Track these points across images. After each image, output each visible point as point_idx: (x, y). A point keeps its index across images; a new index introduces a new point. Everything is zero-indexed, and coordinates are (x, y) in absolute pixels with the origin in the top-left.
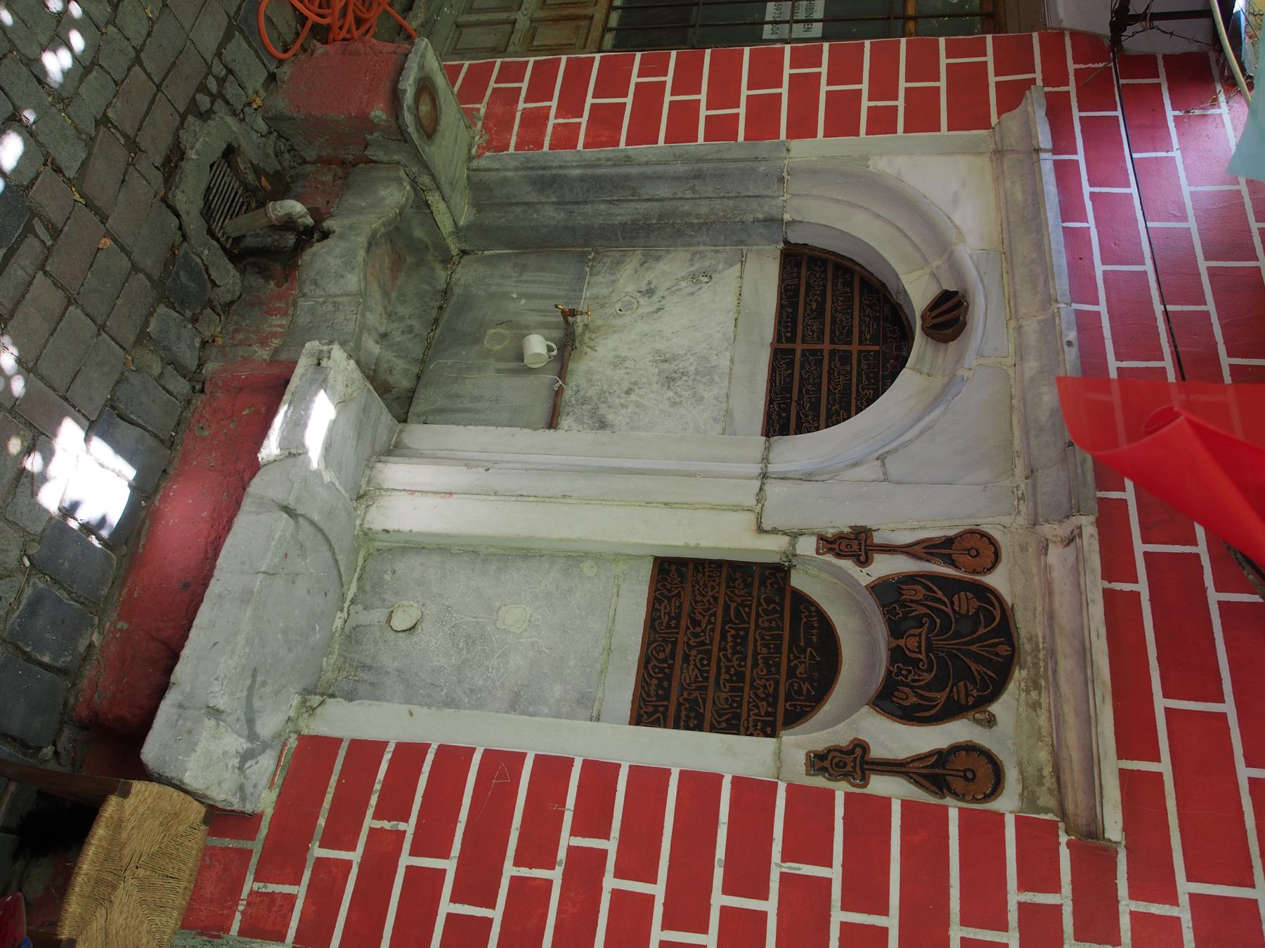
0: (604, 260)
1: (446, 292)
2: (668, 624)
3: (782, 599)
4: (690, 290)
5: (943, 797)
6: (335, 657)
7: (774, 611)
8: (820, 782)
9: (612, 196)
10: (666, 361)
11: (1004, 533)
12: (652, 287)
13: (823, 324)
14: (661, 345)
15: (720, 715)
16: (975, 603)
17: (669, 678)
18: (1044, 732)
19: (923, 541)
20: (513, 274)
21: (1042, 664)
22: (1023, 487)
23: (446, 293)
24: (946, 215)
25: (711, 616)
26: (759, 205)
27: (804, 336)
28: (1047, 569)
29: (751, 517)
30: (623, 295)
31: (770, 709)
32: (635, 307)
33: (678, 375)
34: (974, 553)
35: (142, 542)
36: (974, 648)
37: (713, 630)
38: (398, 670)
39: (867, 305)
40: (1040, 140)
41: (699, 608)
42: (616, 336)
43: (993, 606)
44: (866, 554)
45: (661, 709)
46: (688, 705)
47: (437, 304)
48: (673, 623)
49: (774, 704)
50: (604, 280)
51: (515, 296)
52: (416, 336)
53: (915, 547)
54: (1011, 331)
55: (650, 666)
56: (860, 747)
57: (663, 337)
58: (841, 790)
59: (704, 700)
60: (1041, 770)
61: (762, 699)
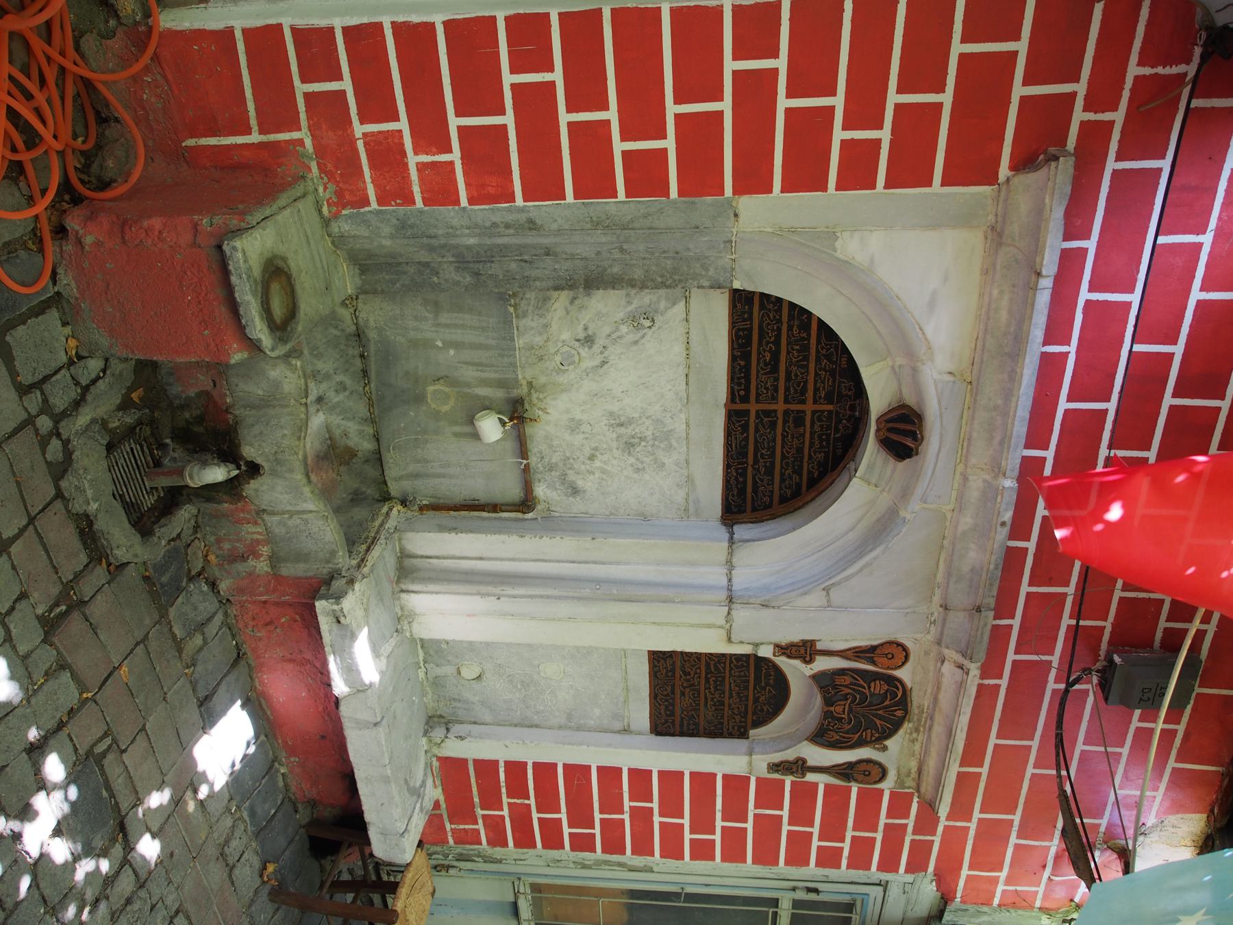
0: (527, 296)
1: (359, 335)
4: (631, 337)
5: (850, 782)
6: (431, 694)
8: (776, 776)
9: (521, 255)
10: (622, 425)
12: (590, 333)
13: (777, 379)
14: (615, 407)
16: (886, 687)
17: (672, 705)
18: (917, 753)
19: (854, 648)
20: (427, 314)
22: (936, 614)
23: (359, 335)
24: (918, 324)
26: (702, 266)
27: (758, 395)
28: (939, 674)
29: (723, 633)
30: (560, 344)
31: (743, 720)
32: (577, 361)
33: (637, 440)
34: (890, 656)
35: (269, 713)
36: (880, 712)
37: (699, 677)
38: (479, 701)
39: (823, 355)
40: (1045, 263)
41: (687, 665)
42: (564, 397)
43: (898, 689)
44: (810, 655)
47: (356, 352)
48: (670, 674)
49: (745, 717)
50: (534, 324)
51: (439, 344)
52: (351, 393)
54: (958, 476)
56: (804, 761)
57: (613, 398)
58: (788, 781)
59: (698, 716)
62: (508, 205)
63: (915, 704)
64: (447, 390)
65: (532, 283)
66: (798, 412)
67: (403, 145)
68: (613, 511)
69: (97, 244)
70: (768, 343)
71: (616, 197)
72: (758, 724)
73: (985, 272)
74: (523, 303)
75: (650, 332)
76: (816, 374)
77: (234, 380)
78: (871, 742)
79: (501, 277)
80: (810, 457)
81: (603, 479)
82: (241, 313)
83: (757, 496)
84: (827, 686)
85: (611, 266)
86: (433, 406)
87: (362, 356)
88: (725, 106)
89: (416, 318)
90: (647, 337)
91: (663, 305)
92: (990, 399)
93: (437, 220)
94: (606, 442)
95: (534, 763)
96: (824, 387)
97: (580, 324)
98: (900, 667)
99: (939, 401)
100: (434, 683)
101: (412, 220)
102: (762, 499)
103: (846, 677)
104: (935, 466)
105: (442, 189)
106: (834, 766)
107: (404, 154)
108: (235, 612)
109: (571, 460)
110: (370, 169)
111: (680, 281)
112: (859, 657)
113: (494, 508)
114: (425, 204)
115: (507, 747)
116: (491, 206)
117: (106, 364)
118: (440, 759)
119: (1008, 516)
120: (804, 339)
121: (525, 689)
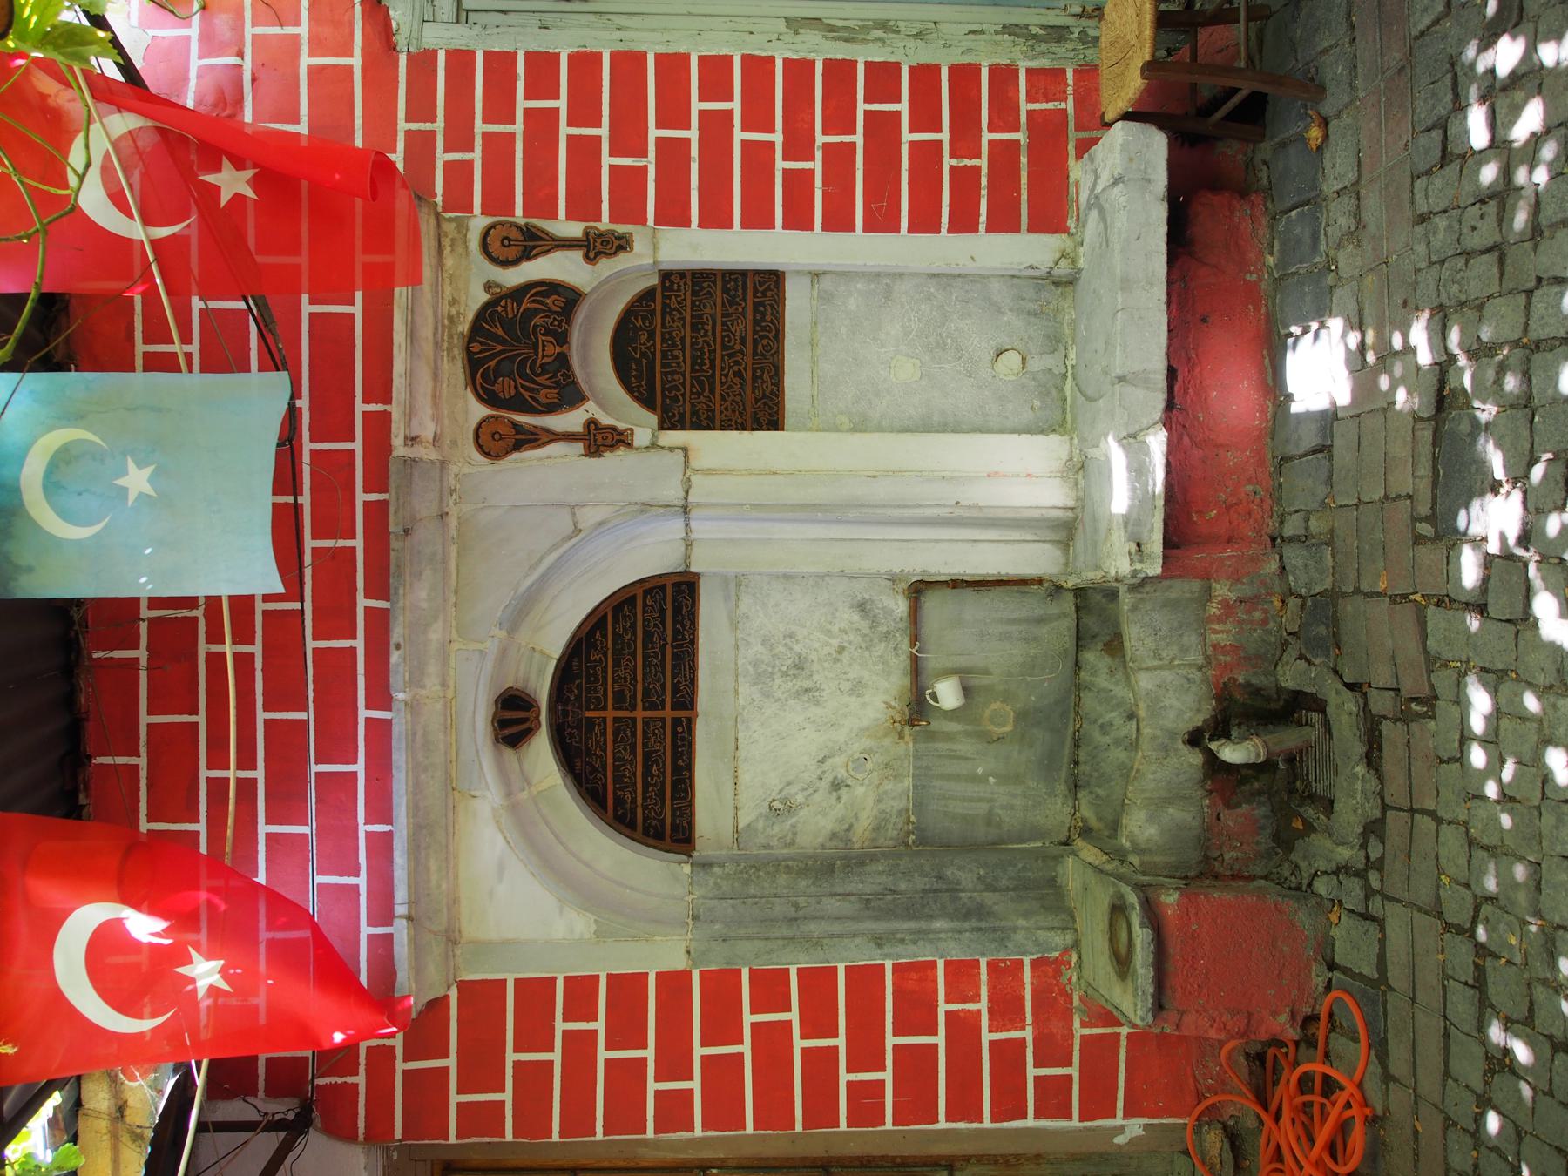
0: (895, 832)
1: (1076, 786)
2: (762, 369)
3: (663, 401)
4: (793, 790)
5: (526, 224)
6: (1066, 321)
7: (670, 390)
8: (621, 229)
9: (894, 899)
10: (806, 690)
11: (470, 458)
12: (835, 794)
13: (645, 745)
14: (815, 711)
15: (709, 293)
16: (496, 387)
17: (756, 323)
18: (447, 281)
19: (539, 446)
20: (1000, 812)
21: (446, 338)
23: (1075, 786)
24: (511, 847)
25: (726, 382)
26: (720, 887)
27: (663, 727)
28: (437, 419)
29: (694, 464)
30: (866, 781)
31: (667, 301)
32: (850, 763)
33: (791, 672)
34: (497, 436)
35: (1267, 360)
36: (499, 348)
37: (723, 369)
38: (1003, 313)
39: (599, 772)
40: (406, 931)
41: (737, 389)
42: (866, 723)
45: (759, 295)
46: (738, 299)
47: (1082, 768)
48: (758, 374)
49: (665, 306)
50: (892, 802)
51: (992, 780)
52: (1096, 721)
53: (546, 440)
54: (452, 684)
55: (774, 332)
56: (590, 259)
57: (814, 721)
58: (605, 223)
60: (452, 251)
61: (675, 309)
62: (900, 961)
63: (459, 363)
64: (991, 727)
65: (887, 869)
66: (620, 708)
67: (990, 1019)
68: (821, 582)
69: (1275, 1013)
70: (655, 785)
71: (798, 969)
72: (647, 296)
73: (456, 901)
74: (900, 826)
75: (774, 795)
76: (605, 751)
77: (1195, 824)
78: (506, 296)
79: (916, 875)
80: (605, 655)
81: (831, 623)
82: (1152, 956)
83: (661, 606)
84: (567, 385)
85: (808, 887)
86: (1008, 708)
87: (1076, 763)
88: (699, 1051)
89: (1012, 807)
90: (776, 790)
91: (761, 824)
92: (432, 777)
93: (969, 947)
94: (824, 669)
95: (938, 231)
96: (596, 734)
97: (845, 804)
98: (483, 421)
99: (481, 768)
100: (1058, 342)
101: (993, 946)
102: (655, 602)
103: (544, 401)
104: (476, 695)
105: (961, 974)
106: (548, 251)
107: (990, 1011)
108: (1271, 524)
109: (864, 645)
110: (1024, 997)
111: (741, 872)
112: (532, 434)
113: (956, 584)
114: (978, 961)
115: (972, 258)
116: (915, 960)
117: (1313, 879)
118: (1066, 230)
119: (395, 657)
120: (621, 789)
121: (941, 337)
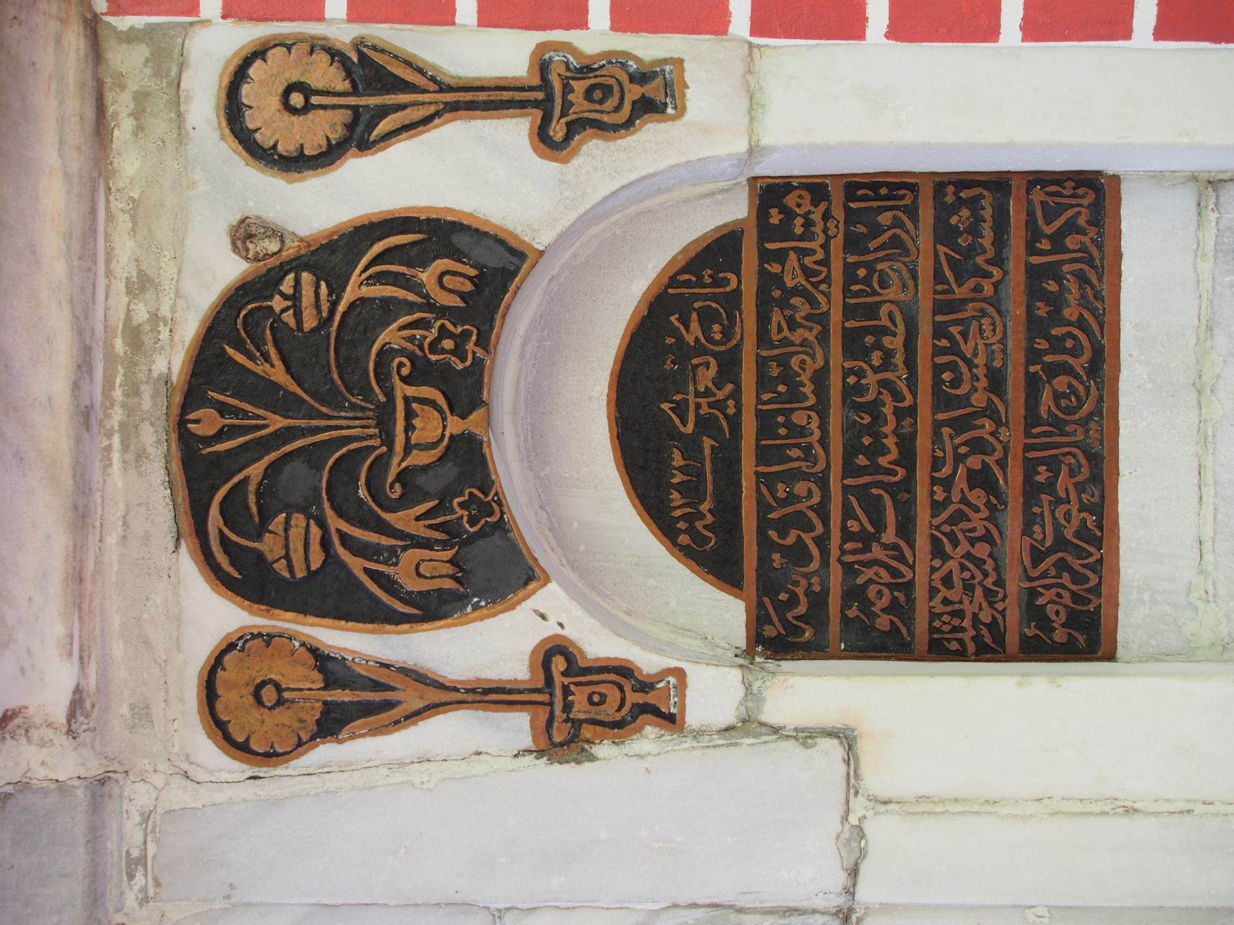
2: (1053, 465)
3: (763, 560)
5: (359, 44)
7: (783, 527)
11: (187, 757)
15: (896, 242)
16: (270, 546)
17: (1035, 326)
18: (124, 223)
19: (397, 724)
21: (118, 394)
22: (131, 900)
25: (947, 502)
29: (875, 780)
31: (775, 268)
34: (269, 694)
36: (277, 422)
37: (936, 464)
41: (978, 522)
43: (224, 540)
44: (549, 681)
45: (1045, 245)
46: (980, 260)
48: (1042, 475)
49: (767, 281)
53: (419, 704)
55: (1087, 355)
59: (938, 277)
60: (139, 129)
61: (797, 291)
63: (156, 472)
78: (297, 264)
84: (482, 534)
103: (412, 585)
112: (377, 686)
